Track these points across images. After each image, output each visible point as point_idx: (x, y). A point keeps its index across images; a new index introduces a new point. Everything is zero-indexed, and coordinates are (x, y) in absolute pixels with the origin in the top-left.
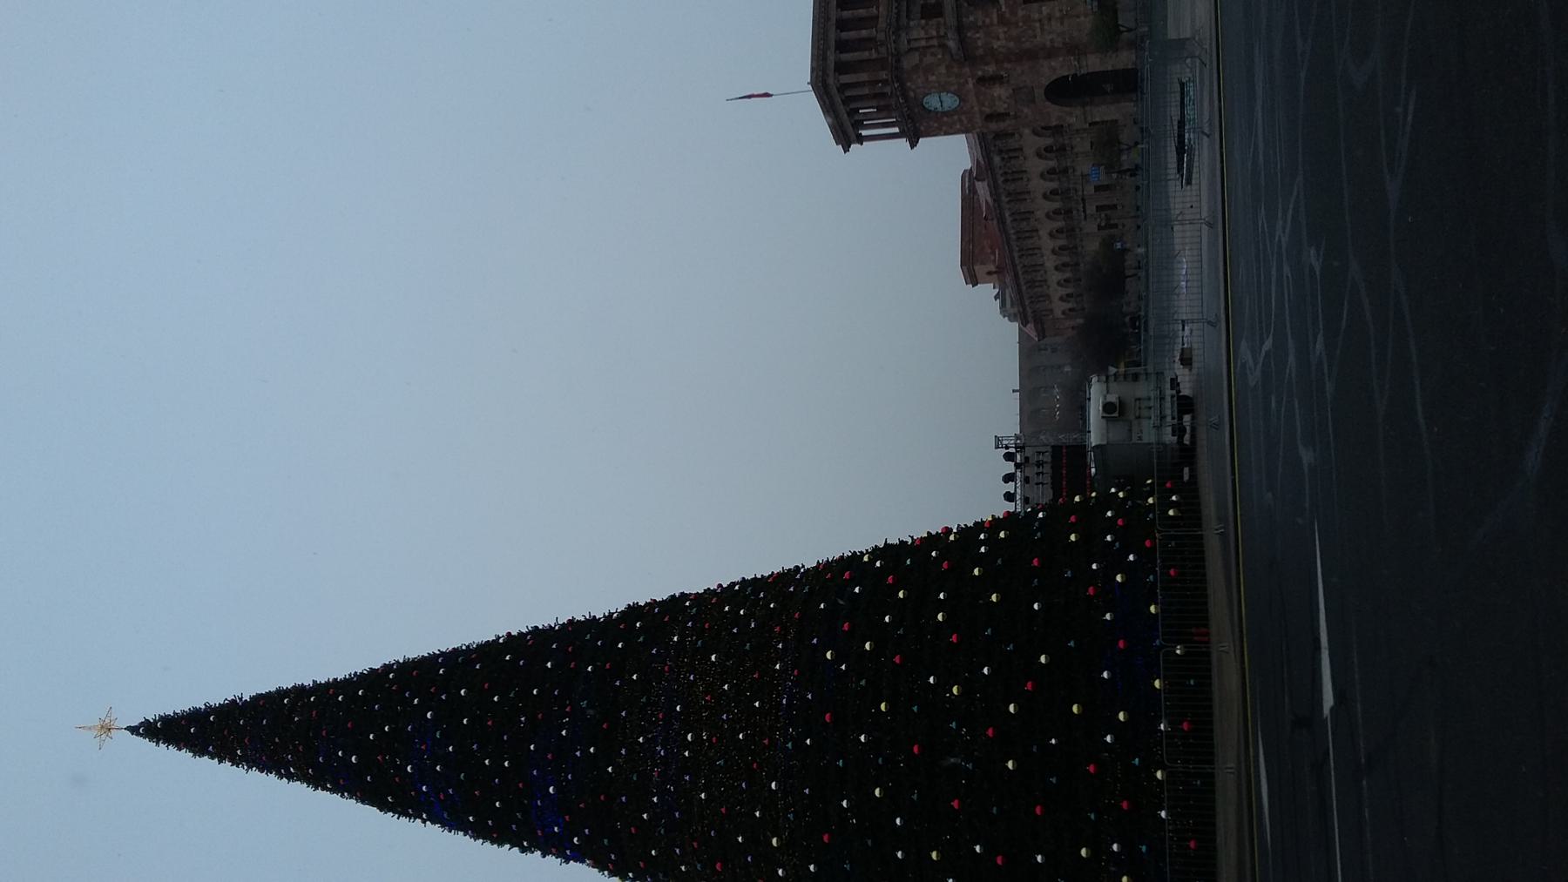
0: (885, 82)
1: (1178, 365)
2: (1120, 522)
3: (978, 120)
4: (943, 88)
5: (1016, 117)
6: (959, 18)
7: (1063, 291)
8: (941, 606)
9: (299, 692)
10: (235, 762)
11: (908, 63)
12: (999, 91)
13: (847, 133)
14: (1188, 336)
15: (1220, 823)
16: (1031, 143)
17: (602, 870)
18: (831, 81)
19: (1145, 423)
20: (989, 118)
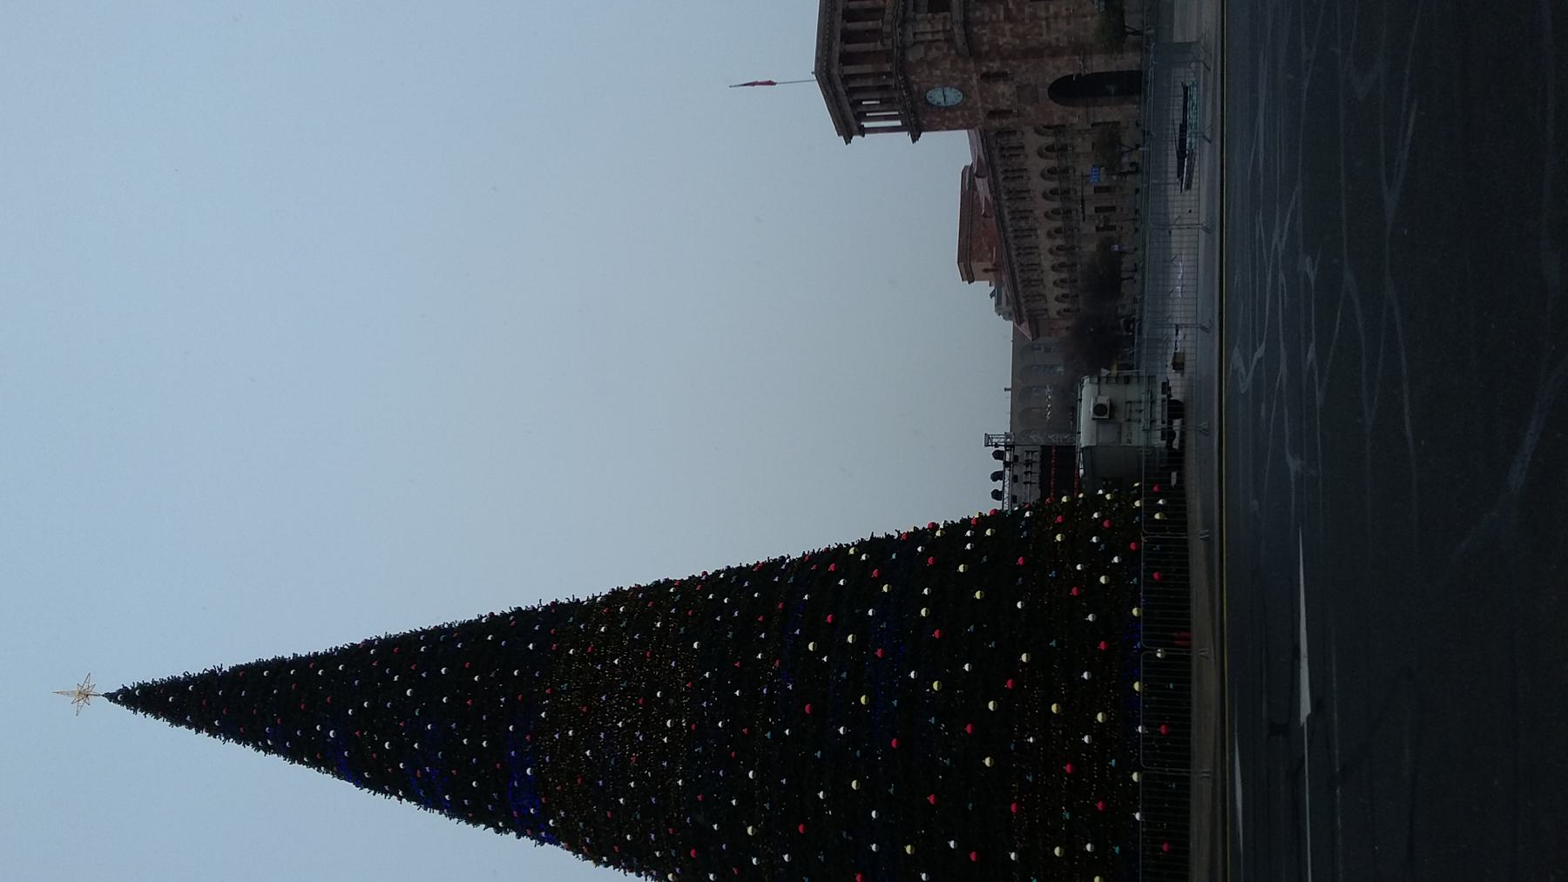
0: (889, 75)
1: (1170, 369)
2: (1106, 524)
3: (981, 116)
4: (945, 84)
5: (1019, 115)
6: (966, 11)
7: (1059, 291)
8: (924, 601)
9: (279, 665)
10: (213, 732)
11: (911, 58)
12: (1001, 88)
13: (849, 125)
14: (1182, 341)
15: (1194, 828)
16: (1033, 141)
17: (576, 853)
18: (835, 71)
19: (1135, 425)
20: (992, 114)
